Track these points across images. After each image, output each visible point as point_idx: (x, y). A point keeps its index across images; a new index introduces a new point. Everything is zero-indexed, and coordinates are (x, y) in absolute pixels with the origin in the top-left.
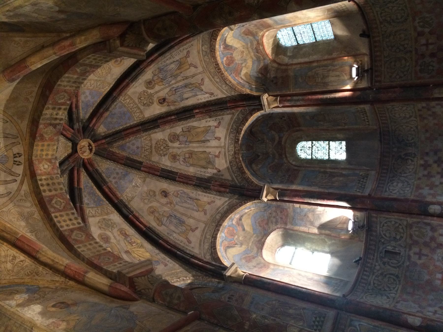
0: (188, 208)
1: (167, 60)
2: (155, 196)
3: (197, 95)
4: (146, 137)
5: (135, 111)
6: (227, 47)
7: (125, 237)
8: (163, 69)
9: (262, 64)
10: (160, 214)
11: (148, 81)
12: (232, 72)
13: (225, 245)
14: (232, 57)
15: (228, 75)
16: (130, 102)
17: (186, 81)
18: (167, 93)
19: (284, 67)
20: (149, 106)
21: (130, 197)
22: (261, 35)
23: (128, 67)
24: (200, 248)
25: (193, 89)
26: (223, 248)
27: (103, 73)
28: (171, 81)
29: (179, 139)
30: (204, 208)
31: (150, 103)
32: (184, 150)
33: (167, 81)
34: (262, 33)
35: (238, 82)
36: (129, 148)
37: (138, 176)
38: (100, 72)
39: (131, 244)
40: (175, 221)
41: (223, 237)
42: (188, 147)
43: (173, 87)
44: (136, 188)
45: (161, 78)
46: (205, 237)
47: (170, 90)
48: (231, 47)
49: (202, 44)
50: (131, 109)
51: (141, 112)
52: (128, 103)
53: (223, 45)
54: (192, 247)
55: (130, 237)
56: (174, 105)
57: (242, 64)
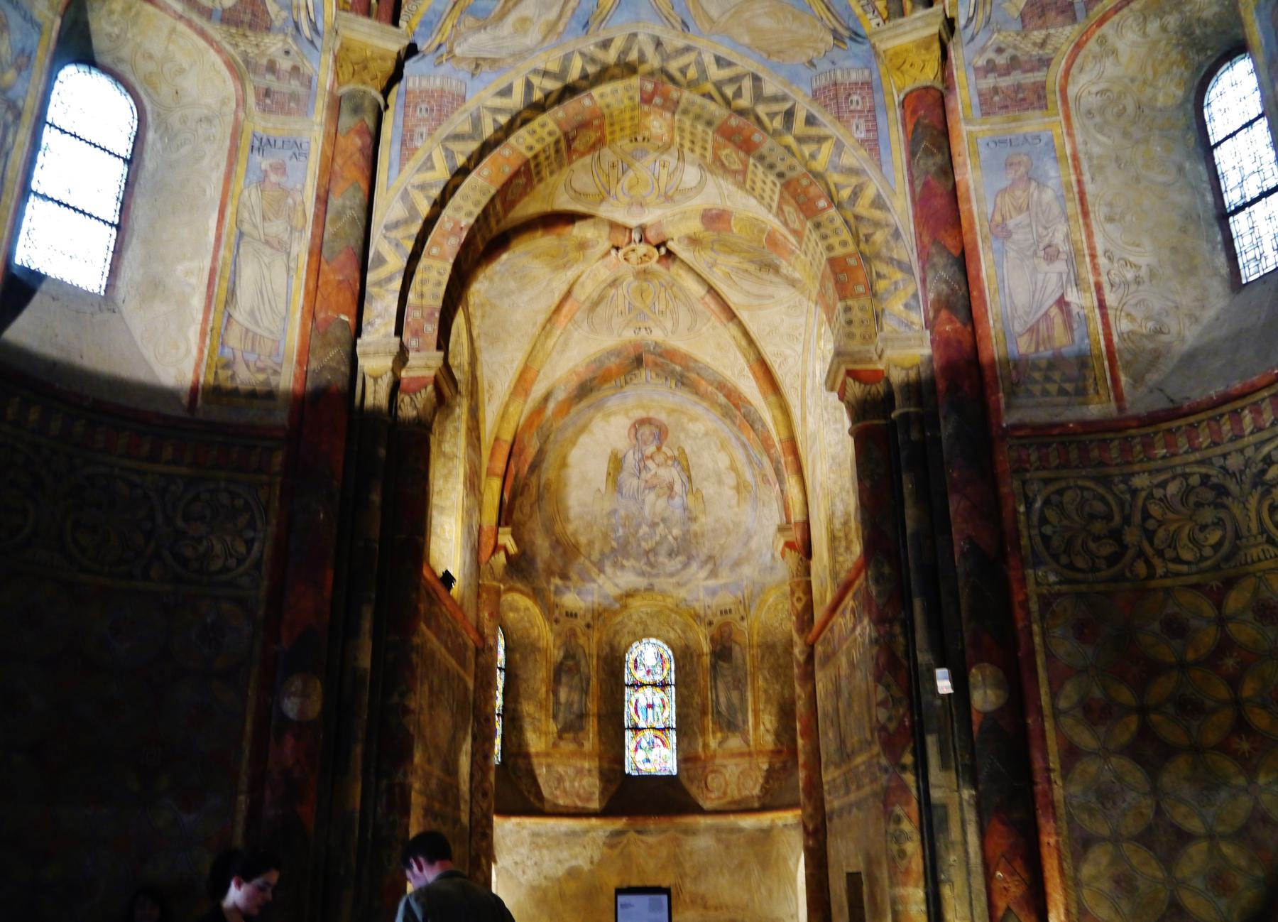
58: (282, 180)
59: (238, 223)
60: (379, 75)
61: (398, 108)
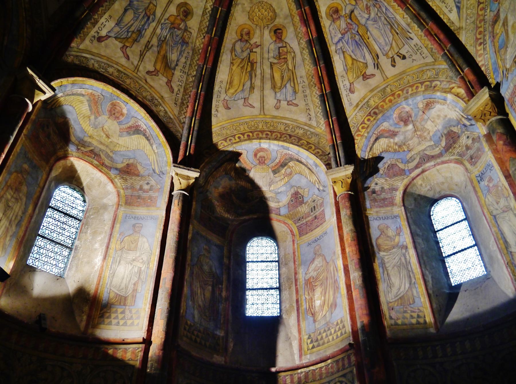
1: (186, 63)
3: (116, 24)
6: (136, 130)
8: (182, 46)
9: (73, 139)
11: (189, 17)
12: (102, 97)
14: (117, 118)
15: (105, 88)
17: (144, 41)
18: (156, 6)
19: (52, 161)
22: (116, 180)
23: (227, 29)
25: (128, 32)
27: (259, 11)
28: (162, 29)
33: (166, 29)
34: (119, 184)
35: (84, 86)
38: (264, 11)
43: (153, 21)
45: (176, 30)
47: (154, 14)
48: (129, 134)
49: (169, 115)
53: (145, 130)
57: (96, 118)
58: (493, 182)
59: (491, 213)
60: (491, 110)
61: (510, 110)
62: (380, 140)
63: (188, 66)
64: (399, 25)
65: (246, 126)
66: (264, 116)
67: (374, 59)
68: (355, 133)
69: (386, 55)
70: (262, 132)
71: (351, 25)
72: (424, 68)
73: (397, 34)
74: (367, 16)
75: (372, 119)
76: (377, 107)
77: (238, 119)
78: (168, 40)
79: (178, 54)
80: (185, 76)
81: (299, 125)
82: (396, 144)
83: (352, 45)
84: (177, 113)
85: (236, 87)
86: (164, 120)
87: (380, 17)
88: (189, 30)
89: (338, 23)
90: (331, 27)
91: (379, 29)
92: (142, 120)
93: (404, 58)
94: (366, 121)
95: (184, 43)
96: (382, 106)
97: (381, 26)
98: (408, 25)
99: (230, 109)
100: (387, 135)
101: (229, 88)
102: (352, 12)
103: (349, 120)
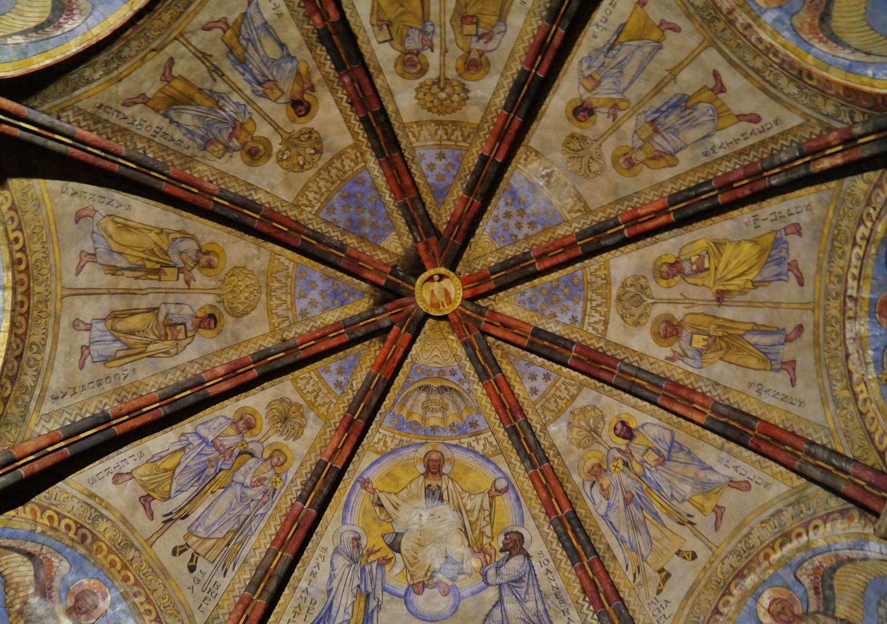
0: (642, 68)
1: (172, 140)
2: (584, 138)
3: (266, 23)
4: (410, 135)
5: (339, 170)
7: (679, 272)
8: (202, 138)
10: (641, 148)
11: (247, 158)
13: (811, 25)
16: (316, 189)
17: (226, 66)
18: (275, 101)
20: (319, 141)
21: (575, 204)
23: (219, 226)
24: (789, 107)
25: (248, 40)
26: (821, 40)
27: (247, 286)
28: (237, 104)
29: (415, 52)
30: (654, 24)
31: (310, 137)
32: (450, 36)
33: (236, 113)
36: (440, 178)
37: (519, 166)
38: (247, 294)
39: (701, 272)
40: (672, 119)
41: (778, 20)
42: (442, 26)
43: (253, 91)
44: (552, 180)
45: (231, 130)
46: (757, 71)
47: (264, 96)
49: (83, 86)
50: (333, 183)
51: (340, 155)
52: (316, 193)
53: (60, 26)
54: (776, 122)
55: (682, 258)
56: (309, 73)
62: (29, 563)
63: (165, 143)
64: (242, 543)
65: (40, 256)
66: (59, 297)
67: (180, 510)
68: (38, 505)
69: (190, 533)
70: (27, 293)
71: (231, 457)
72: (183, 615)
73: (228, 545)
74: (248, 482)
75: (71, 534)
76: (95, 539)
77: (55, 239)
78: (217, 112)
79: (190, 128)
80: (147, 135)
81: (42, 374)
82: (25, 603)
83: (198, 464)
84: (80, 105)
85: (118, 239)
86: (74, 76)
87: (248, 506)
88: (228, 155)
89: (231, 431)
90: (222, 420)
91: (231, 509)
92: (84, 26)
93: (192, 569)
94: (65, 522)
95: (207, 143)
96: (99, 550)
97: (235, 512)
98: (245, 561)
99: (77, 222)
100: (42, 574)
101: (116, 223)
102: (252, 455)
103: (60, 484)
